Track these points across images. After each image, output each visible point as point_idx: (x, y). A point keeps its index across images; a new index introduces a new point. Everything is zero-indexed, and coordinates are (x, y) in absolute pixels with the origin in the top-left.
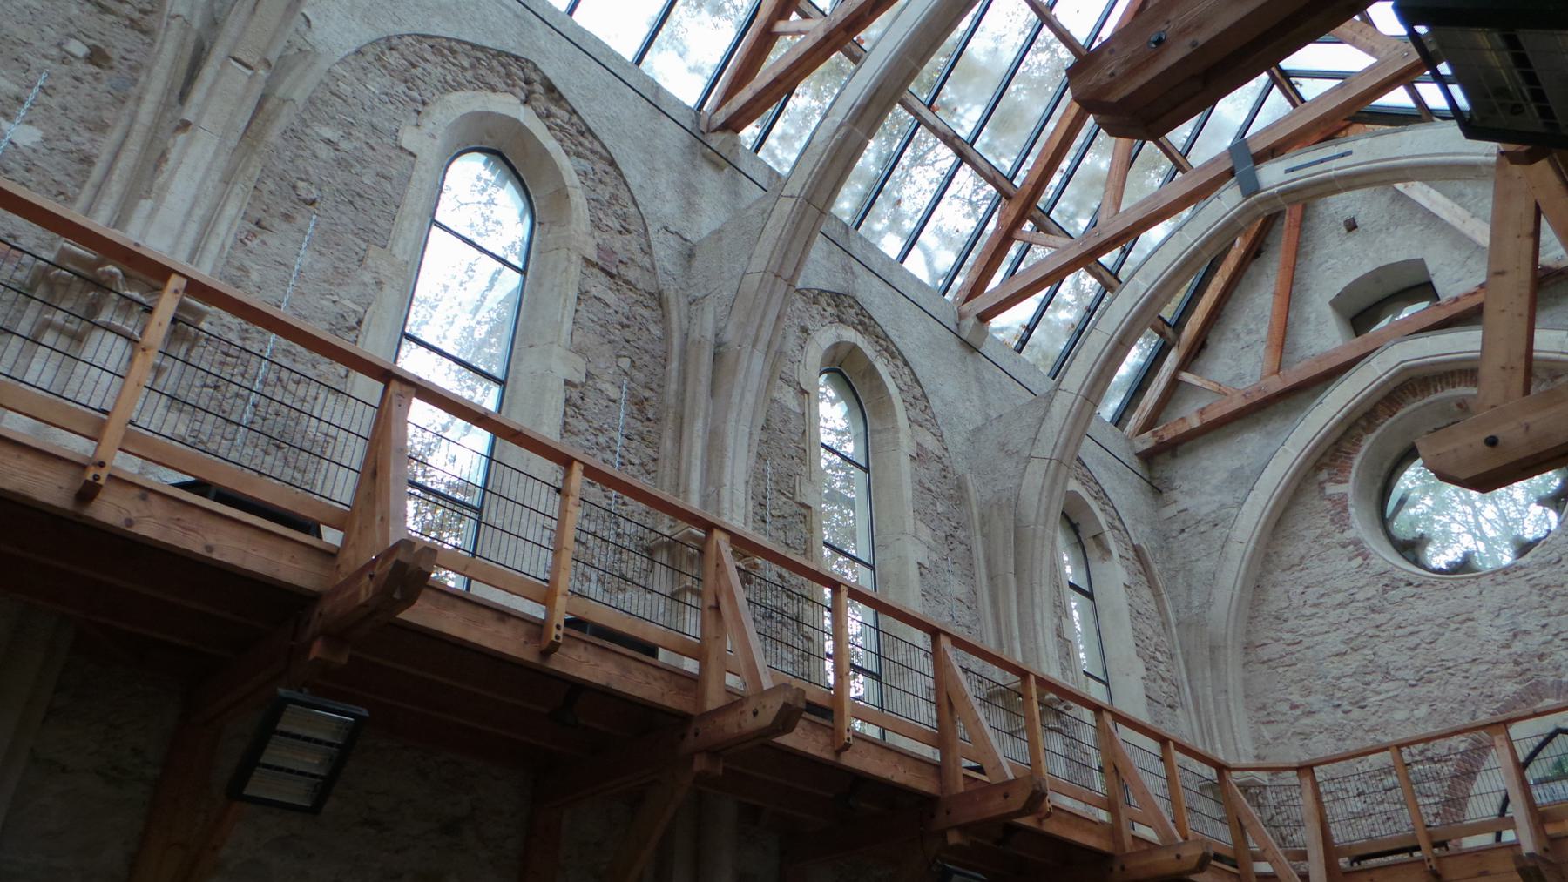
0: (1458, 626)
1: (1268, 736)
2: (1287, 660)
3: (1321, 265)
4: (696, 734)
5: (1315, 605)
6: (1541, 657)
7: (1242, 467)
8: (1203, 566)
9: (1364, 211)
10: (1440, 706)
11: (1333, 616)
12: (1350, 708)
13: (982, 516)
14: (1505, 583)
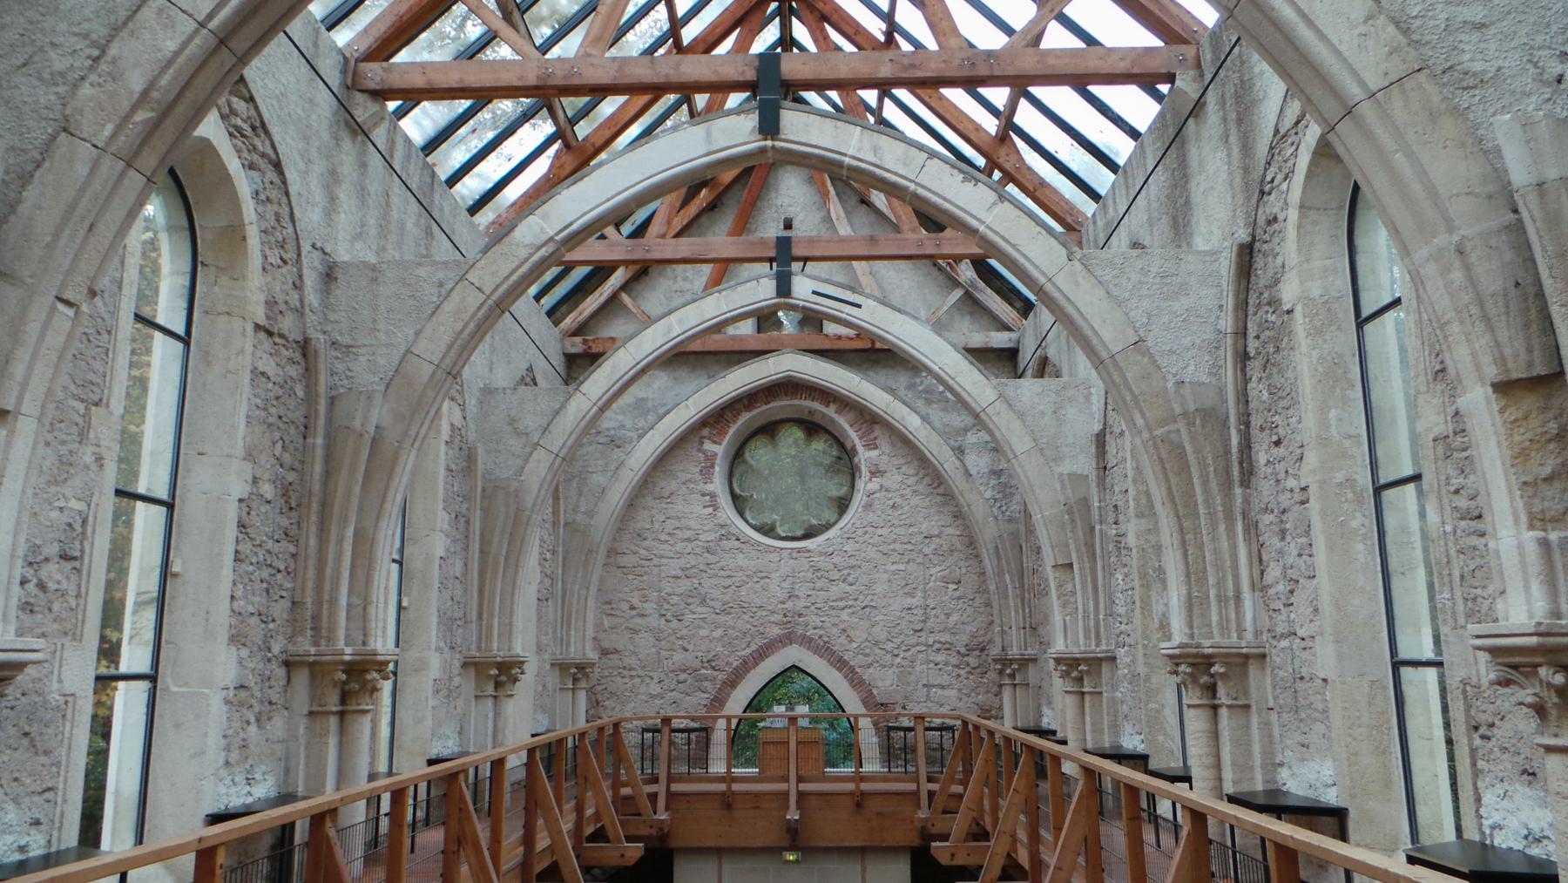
1: (606, 624)
2: (637, 571)
6: (800, 615)
8: (597, 479)
11: (680, 546)
13: (484, 490)
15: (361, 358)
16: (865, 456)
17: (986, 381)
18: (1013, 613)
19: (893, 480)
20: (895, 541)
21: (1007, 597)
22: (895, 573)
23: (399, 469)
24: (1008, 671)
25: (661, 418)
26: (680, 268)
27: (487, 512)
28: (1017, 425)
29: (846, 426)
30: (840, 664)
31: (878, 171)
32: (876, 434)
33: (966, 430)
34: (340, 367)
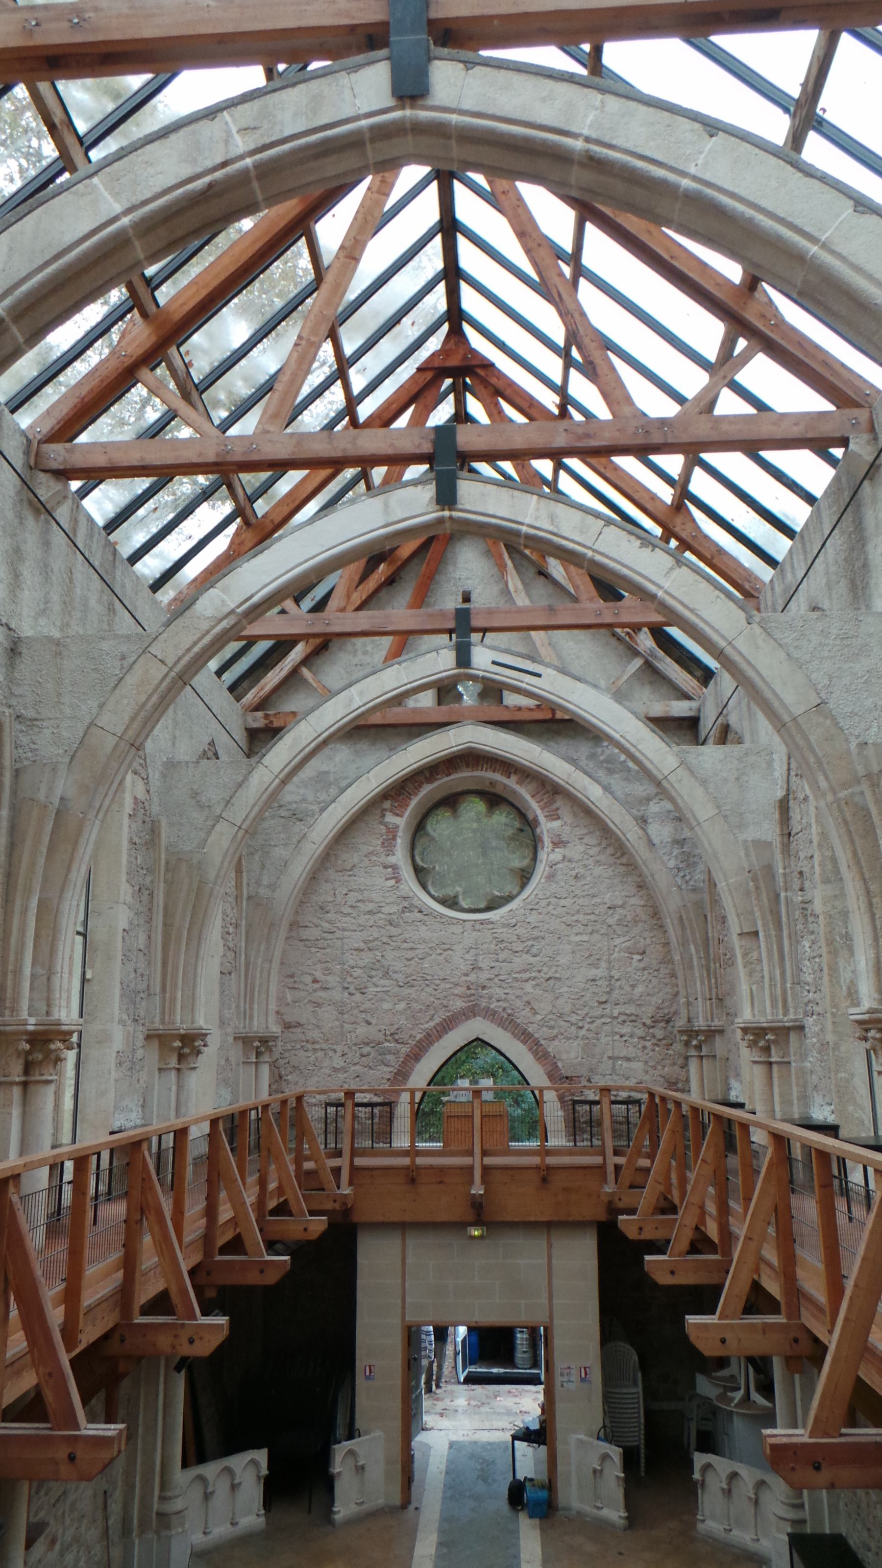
1: (289, 998)
2: (321, 943)
4: (122, 1341)
5: (352, 907)
6: (484, 988)
8: (279, 852)
9: (478, 591)
10: (414, 1005)
11: (362, 919)
13: (167, 863)
15: (46, 731)
16: (547, 827)
17: (668, 749)
18: (698, 984)
19: (576, 850)
20: (578, 912)
21: (691, 967)
22: (578, 944)
23: (83, 840)
24: (694, 1042)
25: (343, 791)
26: (359, 641)
27: (169, 884)
28: (699, 791)
29: (528, 797)
30: (525, 1036)
31: (555, 539)
32: (557, 804)
33: (648, 799)
34: (25, 740)
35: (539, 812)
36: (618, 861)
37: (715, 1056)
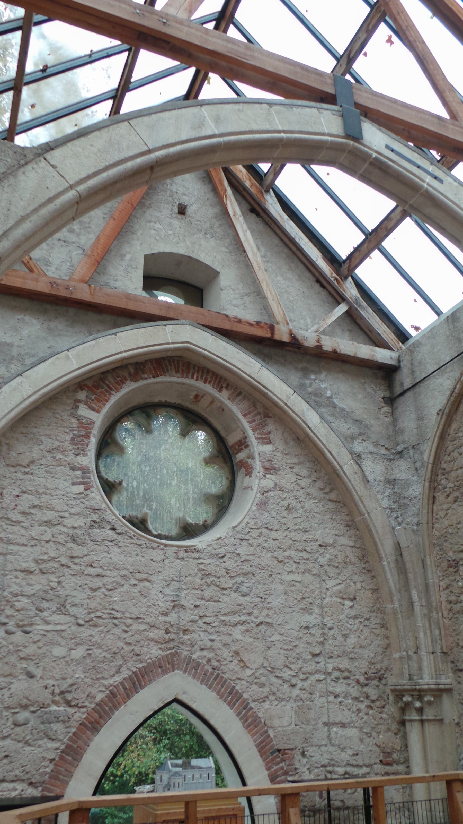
0: (136, 582)
3: (150, 222)
5: (23, 513)
6: (185, 631)
7: (11, 345)
10: (96, 651)
12: (14, 629)
14: (183, 559)
32: (270, 427)
35: (250, 433)
36: (327, 497)
37: (442, 720)
